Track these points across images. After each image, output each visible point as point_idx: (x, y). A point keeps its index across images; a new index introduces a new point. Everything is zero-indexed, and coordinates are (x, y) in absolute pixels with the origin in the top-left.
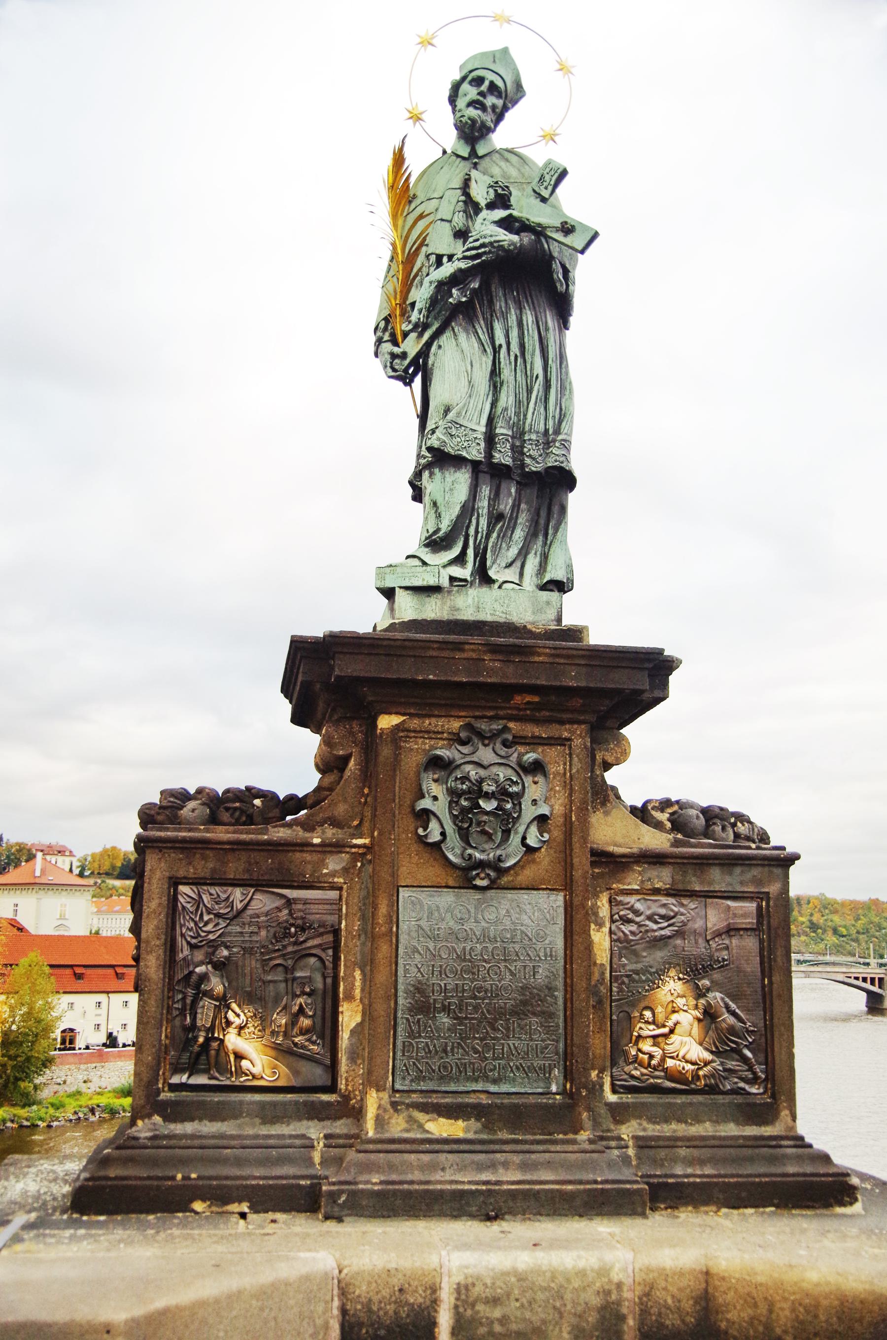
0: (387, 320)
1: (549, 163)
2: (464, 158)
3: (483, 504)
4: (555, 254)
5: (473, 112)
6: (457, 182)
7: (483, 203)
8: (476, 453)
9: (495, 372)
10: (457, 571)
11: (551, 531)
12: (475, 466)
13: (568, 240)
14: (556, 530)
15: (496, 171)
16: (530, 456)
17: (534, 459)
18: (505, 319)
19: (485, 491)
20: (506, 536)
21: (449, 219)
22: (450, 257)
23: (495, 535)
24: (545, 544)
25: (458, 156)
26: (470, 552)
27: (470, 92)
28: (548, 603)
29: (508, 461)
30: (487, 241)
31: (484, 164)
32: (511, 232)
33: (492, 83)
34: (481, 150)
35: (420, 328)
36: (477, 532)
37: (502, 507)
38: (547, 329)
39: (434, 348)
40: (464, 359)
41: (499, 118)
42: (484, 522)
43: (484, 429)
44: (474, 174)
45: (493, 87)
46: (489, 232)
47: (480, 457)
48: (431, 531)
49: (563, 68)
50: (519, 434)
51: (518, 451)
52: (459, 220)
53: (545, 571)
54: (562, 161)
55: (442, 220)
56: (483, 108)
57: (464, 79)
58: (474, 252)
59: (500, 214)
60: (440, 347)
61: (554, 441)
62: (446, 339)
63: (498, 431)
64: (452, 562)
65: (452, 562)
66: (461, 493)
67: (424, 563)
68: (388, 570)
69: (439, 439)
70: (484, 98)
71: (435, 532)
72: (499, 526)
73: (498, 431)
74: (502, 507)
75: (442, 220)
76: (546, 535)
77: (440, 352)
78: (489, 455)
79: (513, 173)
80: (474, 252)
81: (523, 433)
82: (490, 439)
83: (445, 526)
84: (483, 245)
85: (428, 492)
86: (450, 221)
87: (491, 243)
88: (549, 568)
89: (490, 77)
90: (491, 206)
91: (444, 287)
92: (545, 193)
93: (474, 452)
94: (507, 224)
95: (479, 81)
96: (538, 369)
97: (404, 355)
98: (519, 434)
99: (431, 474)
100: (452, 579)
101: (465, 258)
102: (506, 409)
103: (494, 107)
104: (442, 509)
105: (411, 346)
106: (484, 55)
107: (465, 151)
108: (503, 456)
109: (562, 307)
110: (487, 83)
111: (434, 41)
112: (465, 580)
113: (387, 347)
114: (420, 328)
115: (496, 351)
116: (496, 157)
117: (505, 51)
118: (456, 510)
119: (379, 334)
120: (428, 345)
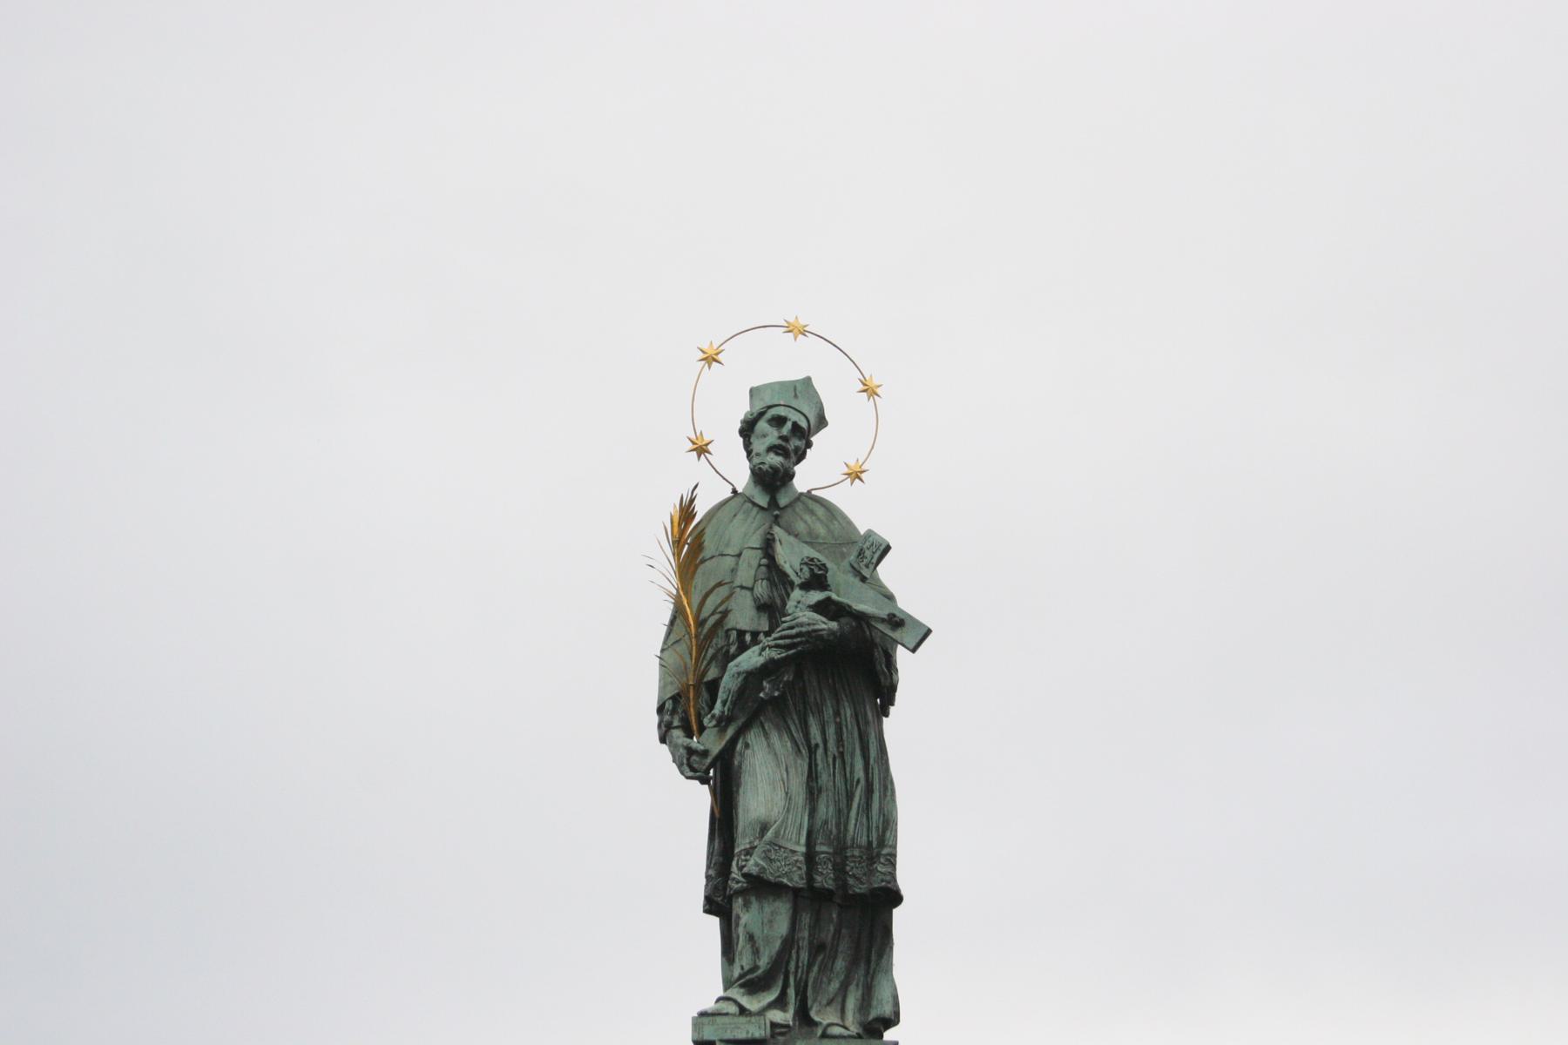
0: (675, 699)
1: (870, 533)
2: (762, 508)
4: (878, 640)
5: (775, 460)
6: (756, 541)
7: (797, 581)
8: (797, 879)
9: (812, 775)
10: (777, 1016)
11: (873, 958)
12: (796, 892)
13: (896, 635)
14: (880, 955)
15: (800, 527)
16: (853, 876)
17: (858, 879)
18: (820, 712)
19: (806, 919)
20: (826, 968)
21: (750, 585)
22: (755, 634)
23: (816, 969)
24: (867, 972)
25: (754, 504)
26: (791, 992)
27: (768, 435)
29: (830, 884)
30: (804, 629)
31: (787, 517)
32: (832, 619)
33: (795, 425)
34: (783, 501)
35: (723, 722)
36: (797, 967)
37: (823, 935)
38: (867, 723)
39: (739, 746)
40: (778, 765)
41: (801, 456)
42: (804, 956)
43: (803, 849)
44: (777, 530)
45: (795, 426)
46: (805, 620)
47: (801, 884)
48: (746, 968)
49: (870, 391)
50: (840, 848)
51: (840, 870)
52: (762, 589)
53: (869, 1005)
54: (886, 533)
55: (742, 587)
57: (761, 414)
58: (788, 641)
59: (816, 596)
60: (747, 746)
61: (879, 855)
62: (754, 737)
63: (818, 848)
66: (782, 927)
67: (743, 1011)
68: (706, 1020)
69: (757, 864)
70: (782, 429)
71: (752, 970)
72: (820, 958)
73: (818, 848)
74: (823, 935)
75: (742, 587)
76: (868, 962)
77: (749, 752)
78: (810, 879)
79: (821, 531)
80: (788, 641)
81: (845, 848)
82: (810, 857)
83: (764, 962)
84: (799, 635)
85: (742, 922)
86: (751, 589)
87: (809, 633)
88: (874, 1003)
89: (794, 417)
90: (806, 587)
91: (753, 678)
92: (866, 572)
93: (796, 878)
94: (823, 608)
95: (779, 421)
96: (859, 773)
97: (705, 753)
98: (840, 848)
99: (747, 905)
100: (774, 1025)
101: (777, 646)
102: (826, 822)
103: (797, 449)
104: (760, 943)
105: (711, 742)
106: (783, 385)
107: (763, 500)
108: (825, 878)
109: (884, 693)
110: (789, 425)
111: (720, 357)
112: (787, 1026)
113: (678, 735)
114: (723, 722)
115: (812, 751)
116: (799, 507)
117: (808, 381)
118: (777, 944)
119: (667, 717)
120: (733, 742)
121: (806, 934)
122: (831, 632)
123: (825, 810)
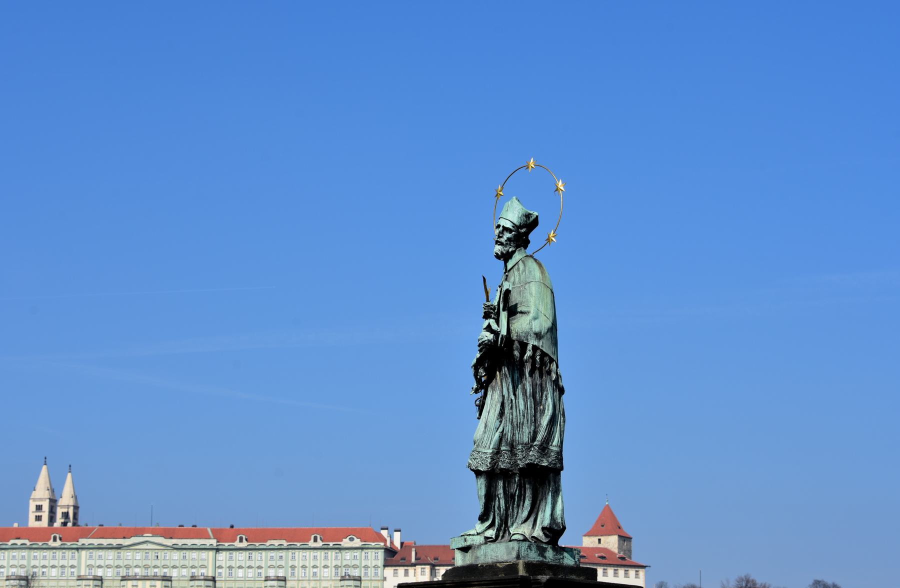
3: (501, 491)
19: (501, 484)
28: (513, 548)
42: (502, 502)
45: (505, 229)
50: (512, 446)
56: (501, 244)
61: (532, 446)
64: (489, 528)
65: (489, 528)
100: (486, 538)
103: (509, 239)
110: (501, 228)
121: (501, 491)
122: (489, 341)
123: (508, 428)
